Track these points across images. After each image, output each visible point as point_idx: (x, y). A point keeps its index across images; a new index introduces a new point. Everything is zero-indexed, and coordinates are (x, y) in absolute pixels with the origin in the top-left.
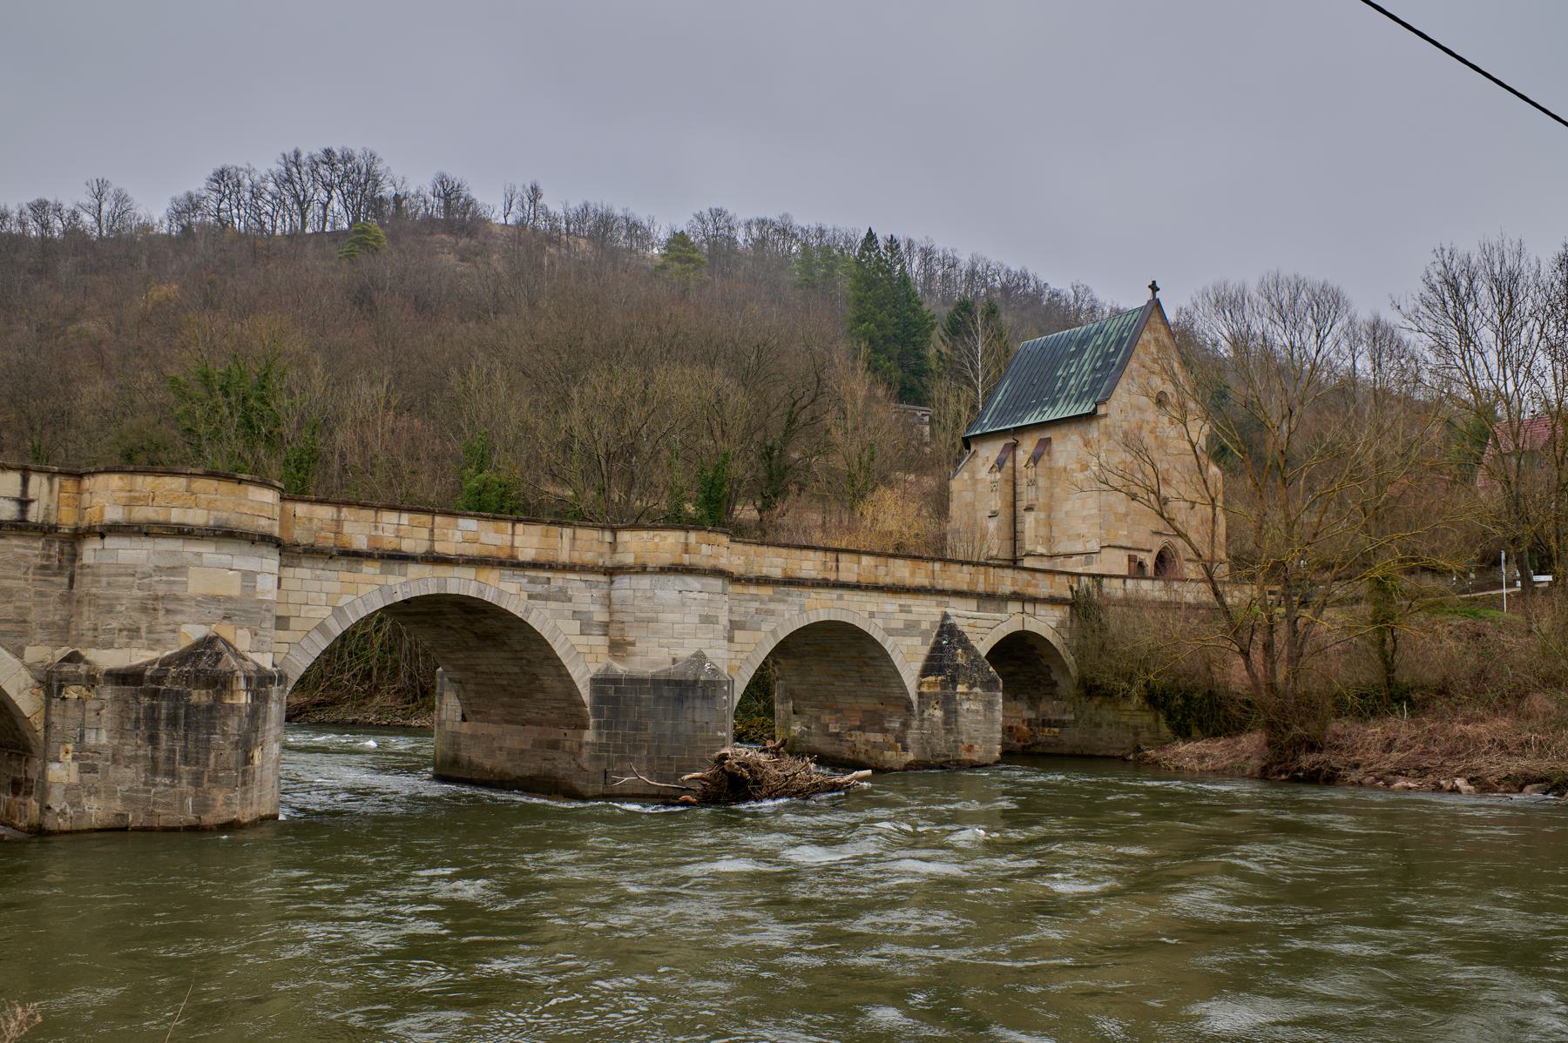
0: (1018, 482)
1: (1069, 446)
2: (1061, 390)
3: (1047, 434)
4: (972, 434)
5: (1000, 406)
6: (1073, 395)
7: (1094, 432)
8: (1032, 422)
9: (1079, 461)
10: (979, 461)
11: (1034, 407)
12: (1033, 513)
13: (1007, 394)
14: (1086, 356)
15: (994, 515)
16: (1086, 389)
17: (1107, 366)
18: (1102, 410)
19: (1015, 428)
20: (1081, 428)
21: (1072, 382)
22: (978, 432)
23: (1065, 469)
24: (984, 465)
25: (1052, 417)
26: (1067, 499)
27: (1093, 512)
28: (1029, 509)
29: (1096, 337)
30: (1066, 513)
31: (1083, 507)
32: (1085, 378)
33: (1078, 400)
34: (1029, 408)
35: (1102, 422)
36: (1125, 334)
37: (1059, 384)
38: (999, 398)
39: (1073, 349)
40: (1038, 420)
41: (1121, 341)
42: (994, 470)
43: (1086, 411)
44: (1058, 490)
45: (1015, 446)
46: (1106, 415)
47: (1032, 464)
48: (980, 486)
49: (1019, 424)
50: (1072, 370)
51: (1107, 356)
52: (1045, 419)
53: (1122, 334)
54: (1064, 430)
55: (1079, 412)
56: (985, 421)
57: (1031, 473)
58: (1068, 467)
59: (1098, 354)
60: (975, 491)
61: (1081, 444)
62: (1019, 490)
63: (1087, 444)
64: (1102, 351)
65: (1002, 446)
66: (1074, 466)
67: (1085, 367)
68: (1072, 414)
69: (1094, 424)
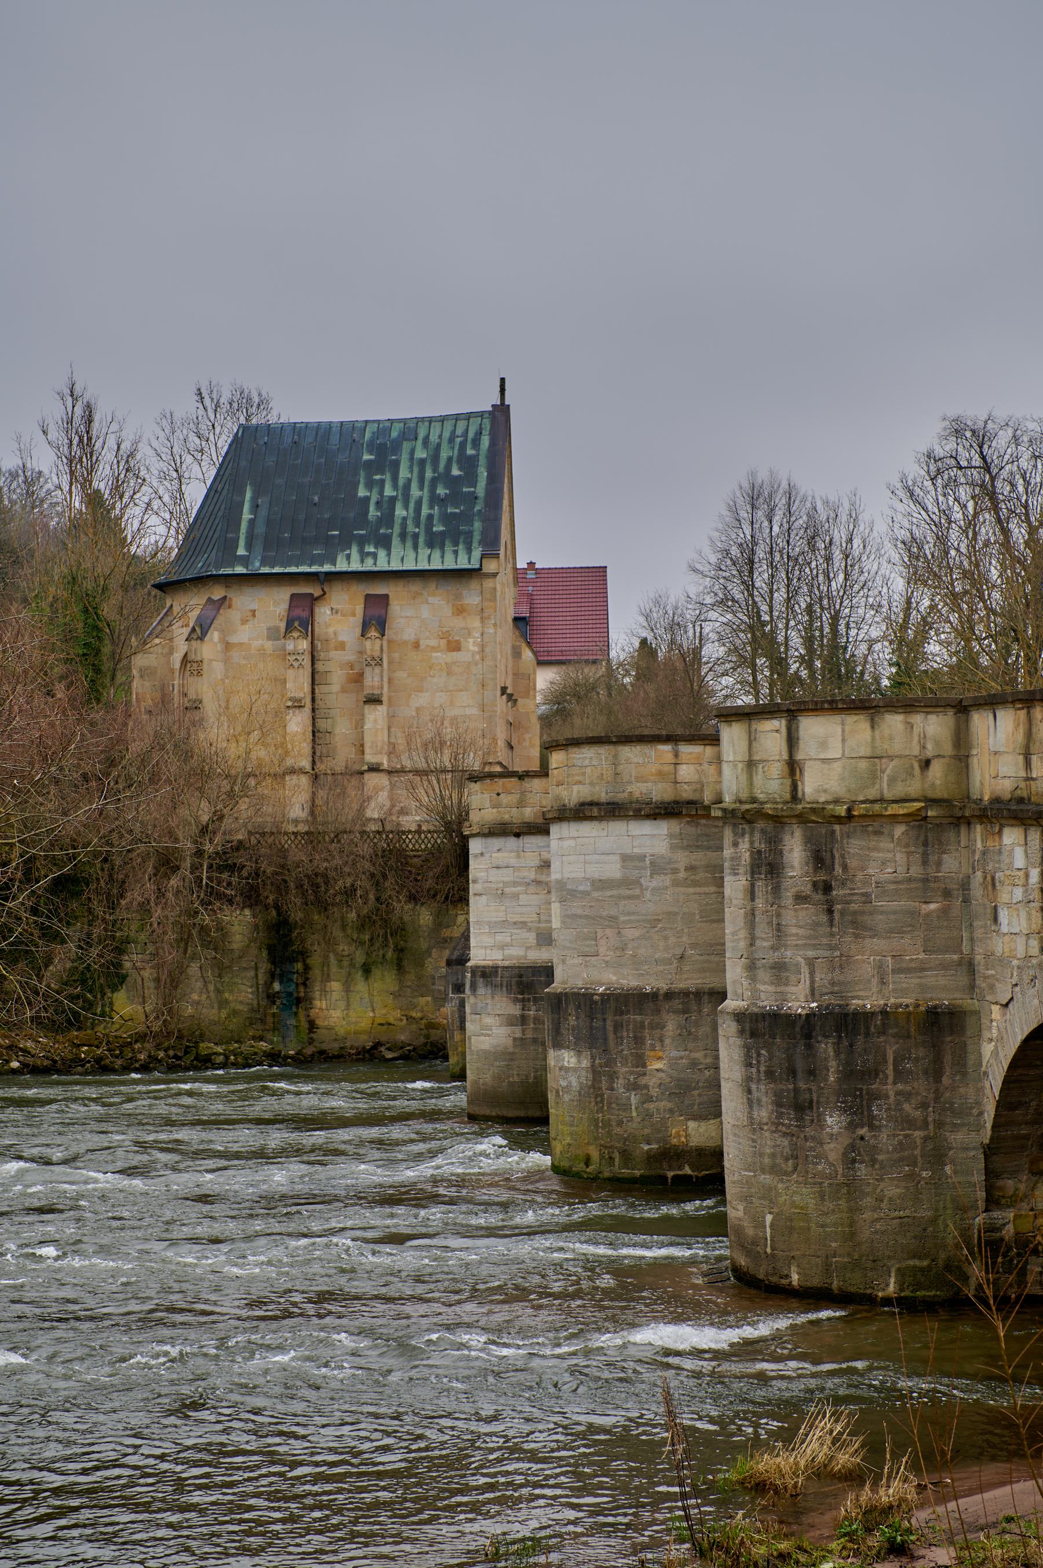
0: (322, 655)
1: (425, 612)
2: (388, 519)
3: (379, 589)
4: (229, 571)
5: (260, 529)
6: (416, 536)
7: (472, 595)
8: (355, 566)
9: (445, 635)
10: (232, 615)
11: (345, 542)
12: (379, 707)
13: (263, 512)
14: (404, 473)
15: (297, 705)
16: (438, 528)
17: (455, 497)
18: (490, 566)
19: (328, 574)
20: (451, 587)
21: (400, 512)
22: (240, 570)
23: (416, 645)
24: (244, 622)
25: (396, 566)
26: (420, 690)
27: (468, 711)
28: (374, 700)
29: (406, 446)
30: (418, 709)
31: (452, 703)
32: (425, 511)
33: (434, 541)
34: (333, 548)
35: (488, 583)
36: (470, 452)
37: (373, 512)
38: (246, 516)
39: (367, 457)
40: (369, 566)
41: (469, 464)
42: (295, 634)
43: (463, 563)
44: (401, 675)
45: (312, 601)
46: (494, 575)
47: (373, 633)
48: (236, 655)
49: (327, 568)
50: (389, 491)
51: (454, 483)
52: (382, 565)
53: (463, 446)
54: (415, 587)
55: (449, 564)
56: (241, 551)
57: (373, 645)
58: (423, 643)
59: (429, 474)
60: (227, 661)
61: (447, 610)
62: (319, 666)
63: (460, 611)
64: (435, 470)
65: (287, 597)
66: (433, 643)
67: (415, 492)
68: (436, 565)
69: (474, 584)
